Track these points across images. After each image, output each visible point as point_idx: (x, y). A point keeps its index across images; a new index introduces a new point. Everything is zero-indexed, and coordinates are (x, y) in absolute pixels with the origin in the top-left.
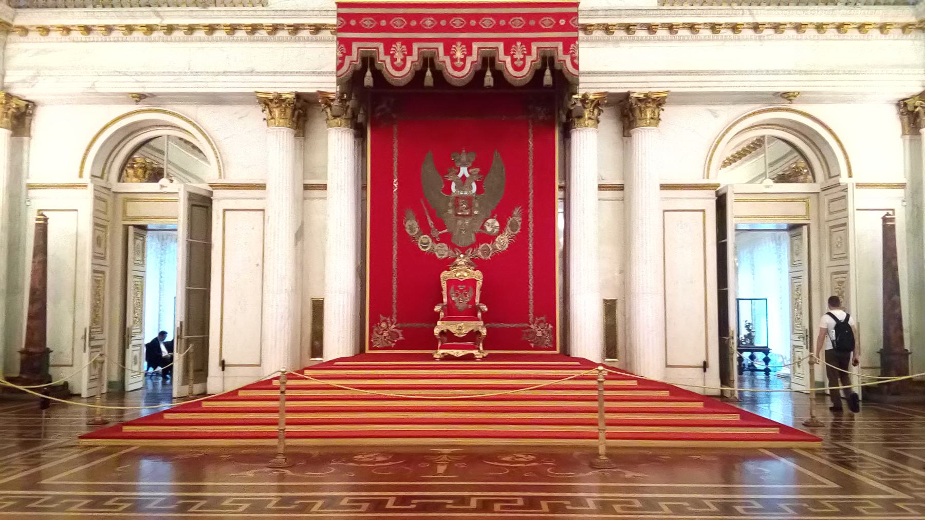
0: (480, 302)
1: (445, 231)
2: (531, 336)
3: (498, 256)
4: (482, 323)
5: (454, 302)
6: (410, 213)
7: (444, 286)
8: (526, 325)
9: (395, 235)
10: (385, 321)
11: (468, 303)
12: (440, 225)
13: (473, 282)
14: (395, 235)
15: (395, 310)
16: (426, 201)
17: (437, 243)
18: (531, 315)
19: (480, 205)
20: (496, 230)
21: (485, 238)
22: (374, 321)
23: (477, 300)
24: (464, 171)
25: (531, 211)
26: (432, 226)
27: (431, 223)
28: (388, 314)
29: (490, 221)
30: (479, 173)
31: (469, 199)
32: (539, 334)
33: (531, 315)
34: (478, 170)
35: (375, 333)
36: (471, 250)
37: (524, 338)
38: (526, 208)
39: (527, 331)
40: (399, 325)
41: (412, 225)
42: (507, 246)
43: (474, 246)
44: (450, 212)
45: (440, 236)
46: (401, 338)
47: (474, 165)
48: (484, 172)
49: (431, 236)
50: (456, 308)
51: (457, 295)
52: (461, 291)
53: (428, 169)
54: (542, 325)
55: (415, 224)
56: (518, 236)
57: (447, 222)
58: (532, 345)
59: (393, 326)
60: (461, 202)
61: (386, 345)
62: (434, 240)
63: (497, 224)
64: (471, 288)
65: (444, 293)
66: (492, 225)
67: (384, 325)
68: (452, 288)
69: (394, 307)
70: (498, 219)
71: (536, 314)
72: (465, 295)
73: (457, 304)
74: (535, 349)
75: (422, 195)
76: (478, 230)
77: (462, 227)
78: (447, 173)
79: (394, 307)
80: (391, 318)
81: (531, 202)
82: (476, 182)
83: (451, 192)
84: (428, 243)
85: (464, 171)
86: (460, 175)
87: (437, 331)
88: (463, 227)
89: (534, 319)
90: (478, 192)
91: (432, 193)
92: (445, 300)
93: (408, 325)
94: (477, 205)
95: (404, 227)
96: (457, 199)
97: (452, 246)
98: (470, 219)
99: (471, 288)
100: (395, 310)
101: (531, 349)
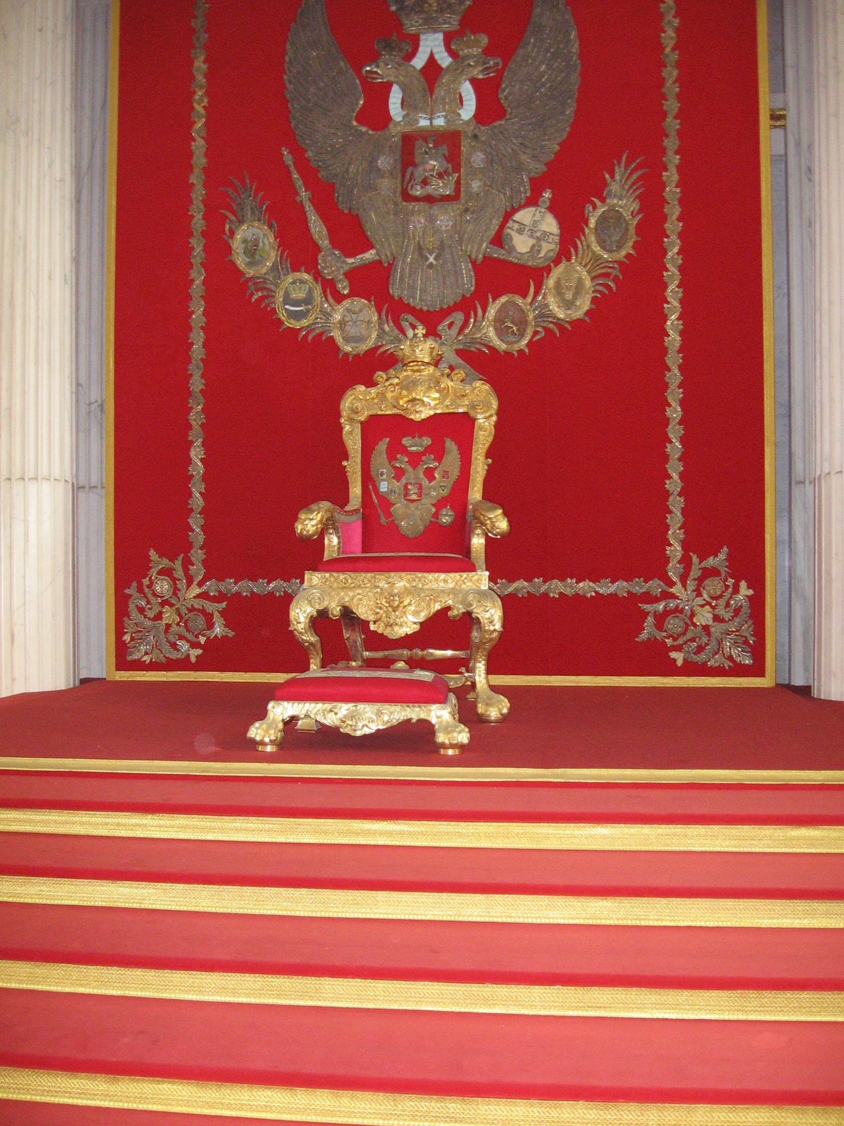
0: (486, 495)
1: (369, 255)
2: (673, 624)
3: (557, 342)
4: (481, 579)
5: (386, 503)
6: (249, 201)
7: (353, 439)
8: (655, 586)
9: (198, 277)
10: (166, 572)
11: (440, 504)
12: (350, 234)
13: (454, 427)
14: (198, 277)
15: (198, 536)
16: (299, 153)
17: (339, 298)
18: (675, 550)
19: (490, 161)
20: (549, 248)
21: (502, 276)
22: (128, 569)
23: (476, 493)
24: (432, 45)
25: (671, 176)
26: (324, 242)
27: (317, 227)
28: (176, 545)
29: (525, 216)
30: (487, 52)
31: (450, 142)
32: (704, 617)
33: (675, 550)
34: (484, 40)
35: (134, 613)
36: (458, 317)
37: (648, 630)
38: (657, 166)
39: (661, 607)
40: (211, 586)
41: (253, 241)
42: (584, 304)
43: (468, 306)
44: (387, 186)
45: (350, 275)
46: (219, 630)
47: (470, 22)
48: (503, 47)
49: (317, 276)
50: (394, 527)
51: (399, 474)
52: (415, 459)
53: (309, 49)
54: (713, 586)
55: (267, 239)
56: (627, 267)
57: (372, 221)
58: (678, 657)
59: (195, 591)
60: (420, 148)
61: (174, 655)
62: (329, 287)
63: (550, 225)
64: (451, 446)
65: (353, 467)
66: (534, 231)
67: (163, 586)
68: (383, 445)
69: (196, 522)
70: (553, 209)
71: (698, 543)
72: (429, 474)
73: (399, 507)
74: (691, 669)
75: (290, 139)
76: (482, 248)
77: (429, 248)
78: (374, 58)
79: (196, 522)
80: (187, 563)
81: (671, 143)
82: (474, 82)
83: (390, 119)
84: (308, 300)
85: (432, 45)
86: (419, 62)
87: (300, 615)
88: (430, 241)
89: (686, 561)
90: (480, 117)
91: (326, 131)
92: (356, 491)
93: (246, 587)
94: (478, 159)
95: (229, 250)
96: (409, 141)
97: (395, 310)
98: (454, 209)
99: (451, 446)
100: (198, 536)
101: (671, 670)
